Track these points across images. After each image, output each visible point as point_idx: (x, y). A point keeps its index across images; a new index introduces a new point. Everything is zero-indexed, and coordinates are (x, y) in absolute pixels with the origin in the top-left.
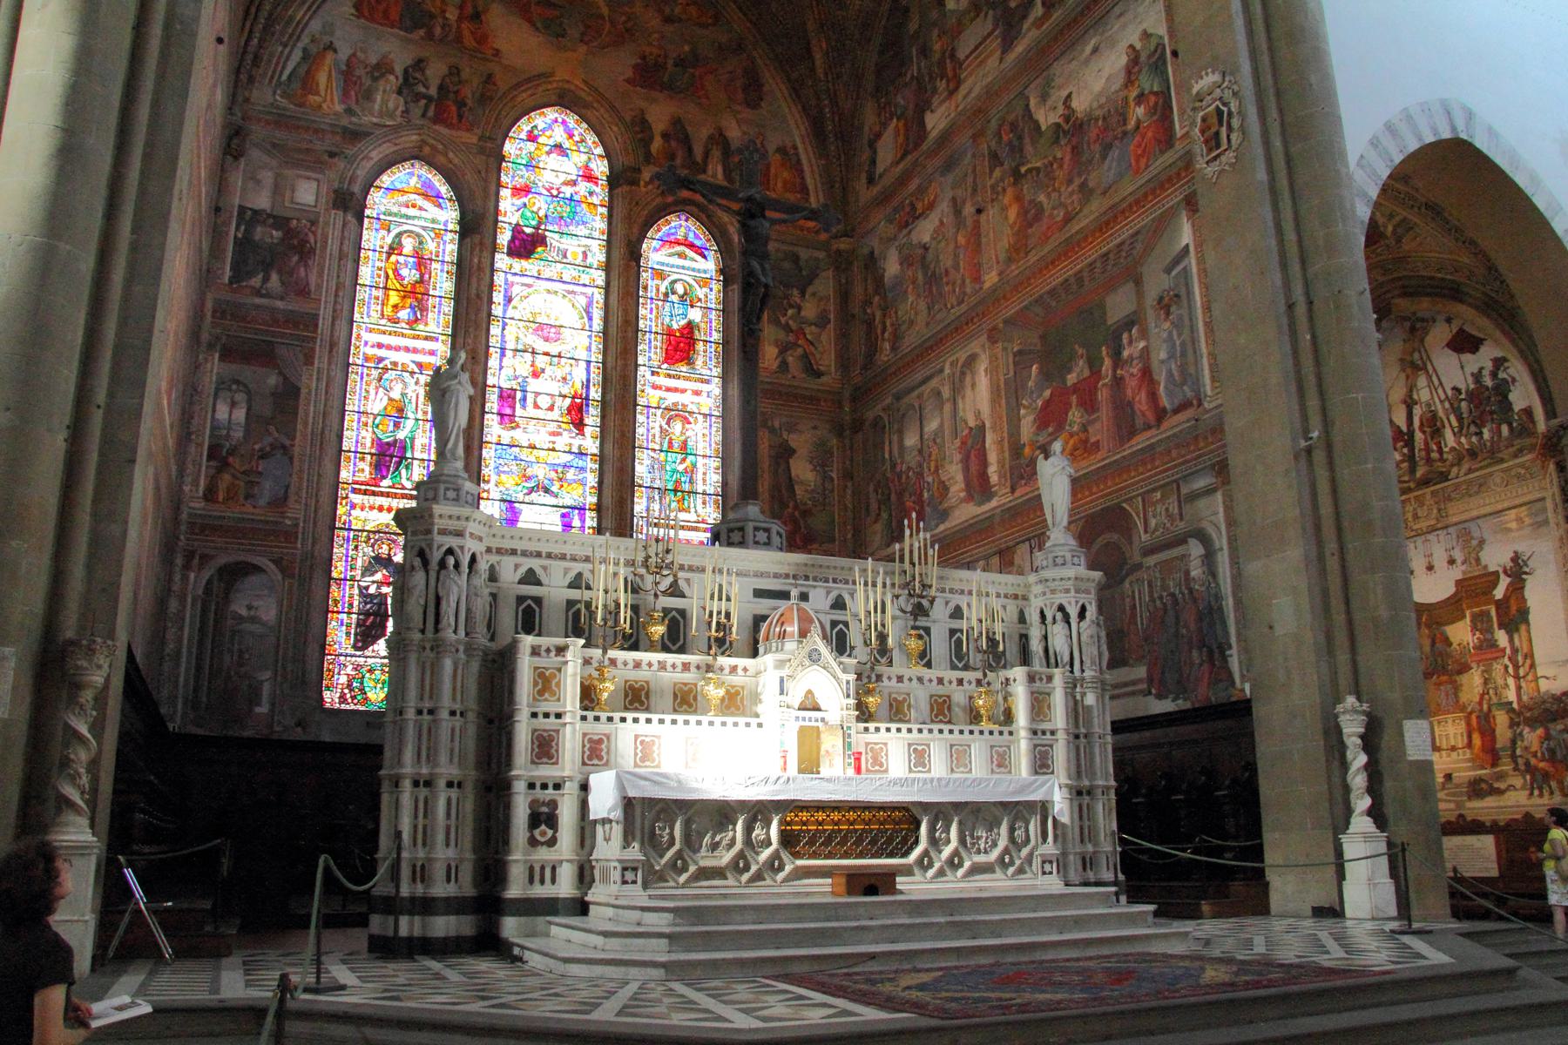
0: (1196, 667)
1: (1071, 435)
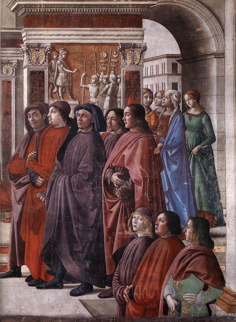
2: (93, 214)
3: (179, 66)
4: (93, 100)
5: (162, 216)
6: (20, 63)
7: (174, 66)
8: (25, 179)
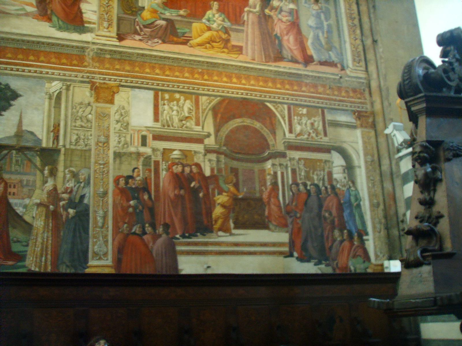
0: (337, 243)
1: (209, 29)
2: (320, 230)
3: (346, 171)
4: (316, 182)
5: (345, 231)
6: (287, 165)
7: (344, 170)
8: (292, 214)
